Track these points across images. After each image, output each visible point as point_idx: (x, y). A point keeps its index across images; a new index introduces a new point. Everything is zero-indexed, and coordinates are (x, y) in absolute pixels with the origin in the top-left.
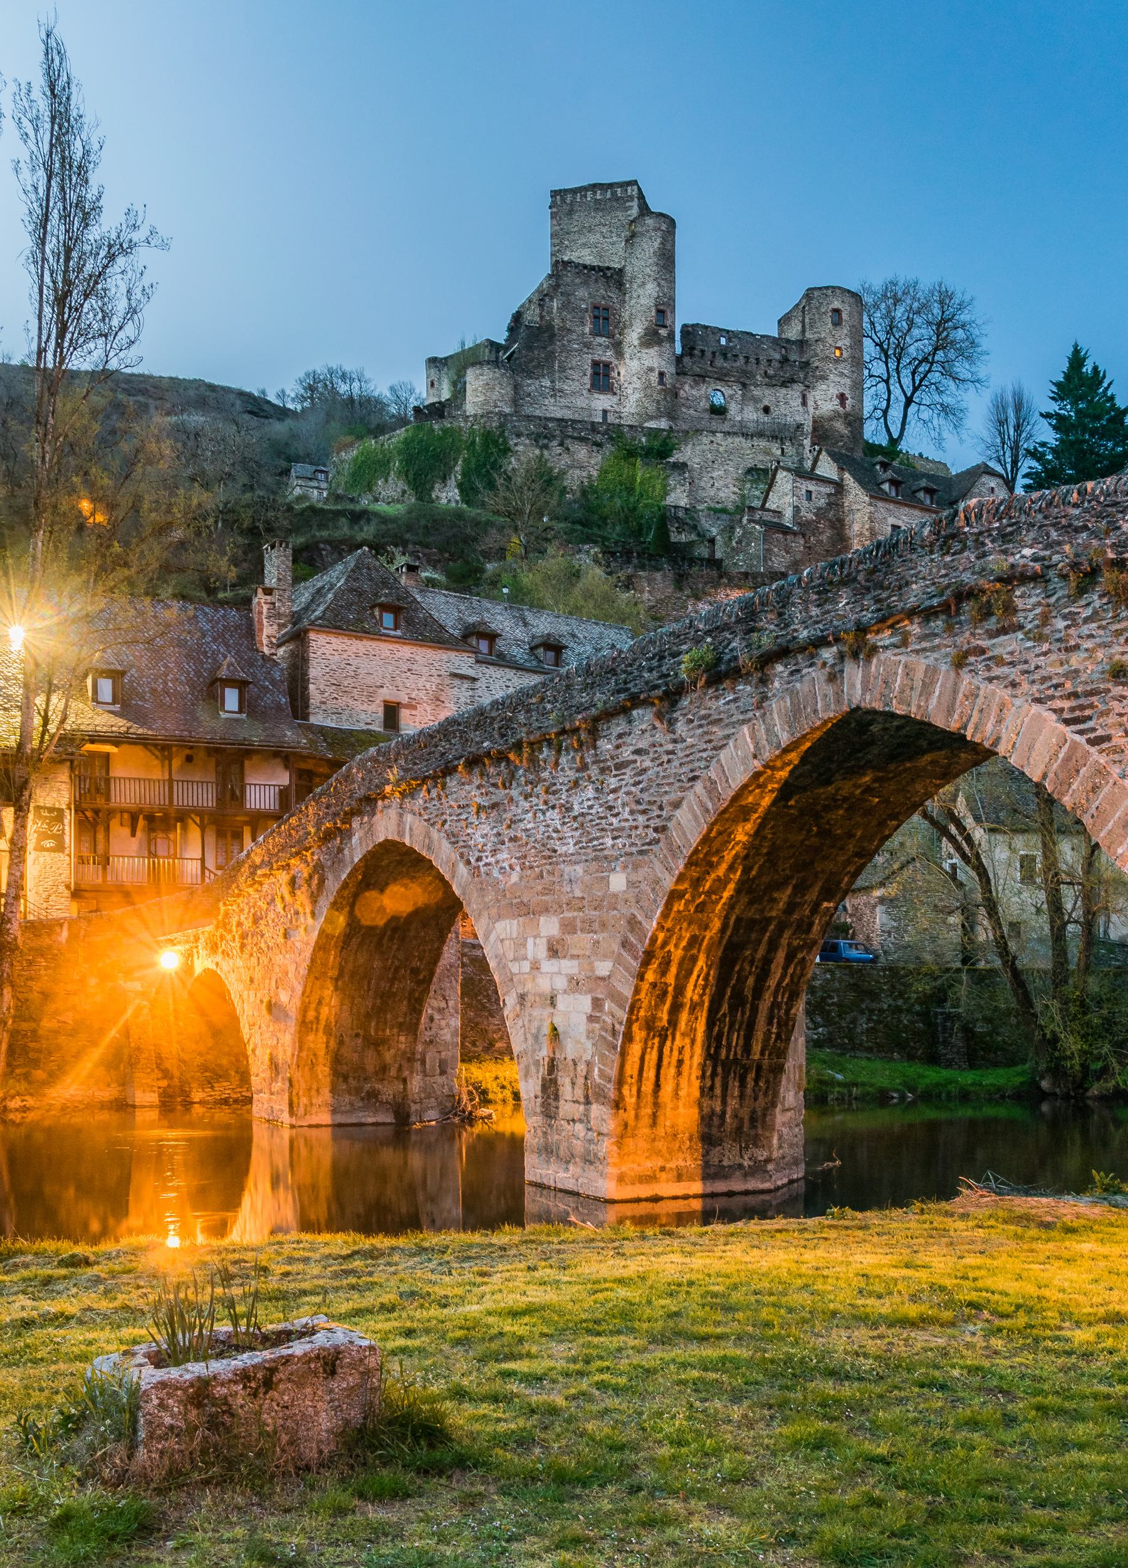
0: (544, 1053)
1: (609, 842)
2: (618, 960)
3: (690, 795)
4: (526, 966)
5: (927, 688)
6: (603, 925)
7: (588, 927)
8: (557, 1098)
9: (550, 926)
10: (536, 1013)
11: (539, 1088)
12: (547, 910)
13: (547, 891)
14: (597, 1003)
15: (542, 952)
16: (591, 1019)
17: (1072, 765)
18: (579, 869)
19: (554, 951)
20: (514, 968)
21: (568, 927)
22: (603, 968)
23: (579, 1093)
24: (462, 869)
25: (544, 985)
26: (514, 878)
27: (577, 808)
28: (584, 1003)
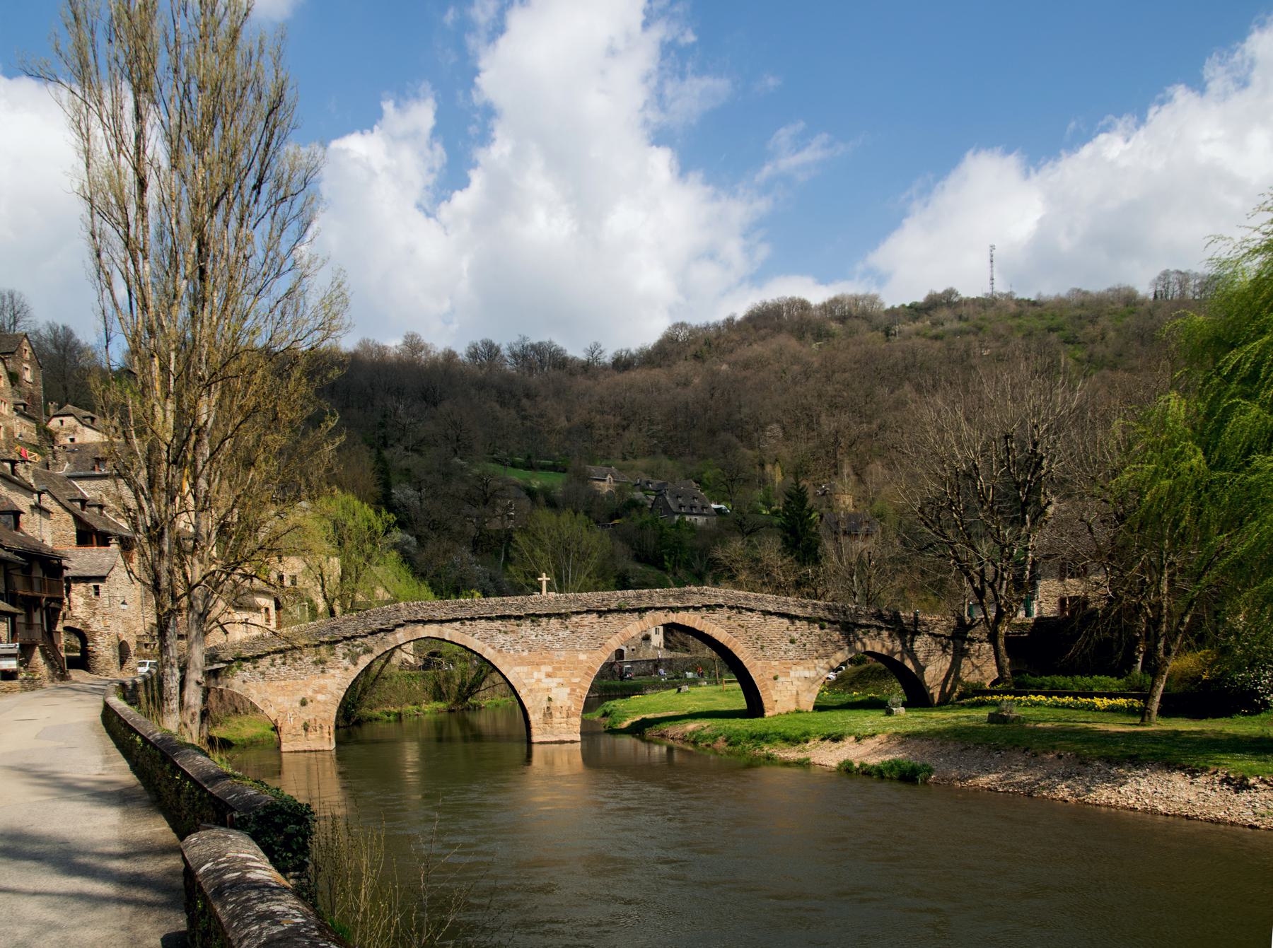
0: (545, 706)
1: (577, 646)
2: (584, 678)
3: (615, 637)
4: (533, 681)
5: (694, 622)
6: (575, 669)
7: (567, 668)
8: (551, 717)
9: (549, 669)
10: (540, 694)
11: (541, 716)
12: (545, 663)
13: (545, 658)
14: (573, 690)
15: (542, 676)
16: (569, 694)
17: (730, 641)
18: (563, 653)
19: (549, 675)
20: (526, 681)
21: (554, 668)
22: (577, 680)
23: (565, 716)
24: (489, 649)
25: (543, 685)
26: (526, 653)
27: (561, 636)
28: (568, 690)
